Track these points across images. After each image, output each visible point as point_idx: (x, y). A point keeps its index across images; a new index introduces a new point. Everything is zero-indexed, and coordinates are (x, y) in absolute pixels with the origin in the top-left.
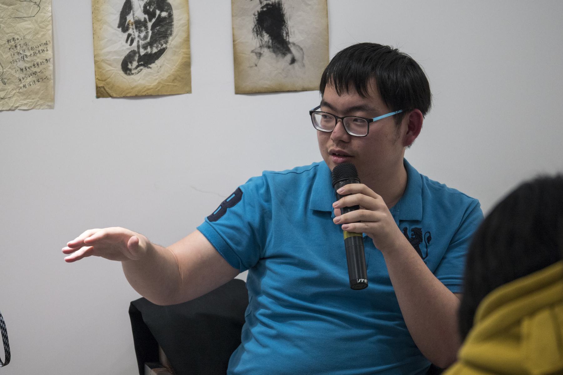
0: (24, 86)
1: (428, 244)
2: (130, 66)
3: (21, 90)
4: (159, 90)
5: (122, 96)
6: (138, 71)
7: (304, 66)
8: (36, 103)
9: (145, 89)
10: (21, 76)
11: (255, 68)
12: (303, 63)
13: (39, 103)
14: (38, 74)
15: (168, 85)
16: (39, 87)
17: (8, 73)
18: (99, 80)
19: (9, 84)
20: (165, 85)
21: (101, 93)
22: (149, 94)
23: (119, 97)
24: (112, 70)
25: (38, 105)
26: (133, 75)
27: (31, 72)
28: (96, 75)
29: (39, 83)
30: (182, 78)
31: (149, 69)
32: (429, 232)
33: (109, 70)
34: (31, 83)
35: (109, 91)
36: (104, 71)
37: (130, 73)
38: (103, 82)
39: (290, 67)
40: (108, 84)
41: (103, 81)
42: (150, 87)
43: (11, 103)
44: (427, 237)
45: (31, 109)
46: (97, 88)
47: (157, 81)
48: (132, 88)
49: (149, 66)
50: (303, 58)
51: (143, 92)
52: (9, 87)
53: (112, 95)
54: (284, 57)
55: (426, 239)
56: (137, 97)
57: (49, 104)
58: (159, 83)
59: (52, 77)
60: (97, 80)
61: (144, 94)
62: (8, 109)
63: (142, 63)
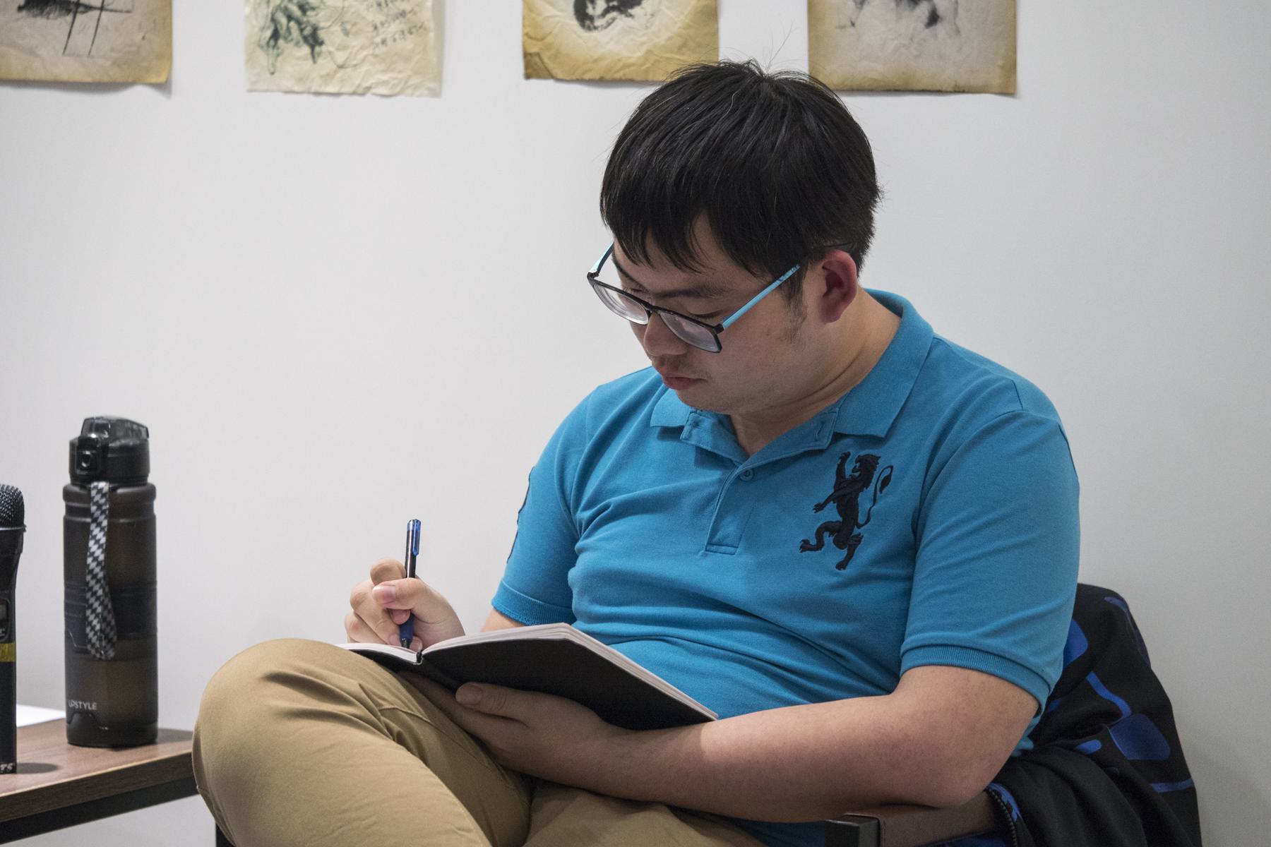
0: (384, 42)
1: (878, 493)
2: (590, 10)
3: (377, 51)
4: (648, 68)
5: (574, 78)
6: (607, 22)
7: (958, 32)
8: (406, 82)
9: (621, 64)
10: (379, 18)
11: (851, 30)
12: (955, 24)
13: (411, 82)
14: (409, 16)
15: (667, 59)
16: (410, 47)
17: (352, 10)
18: (531, 38)
19: (356, 34)
20: (661, 57)
21: (534, 68)
22: (629, 77)
23: (568, 79)
24: (556, 16)
25: (409, 86)
26: (596, 31)
27: (396, 11)
28: (524, 26)
29: (412, 36)
30: (699, 45)
31: (629, 19)
32: (892, 467)
33: (549, 17)
34: (397, 36)
35: (550, 65)
36: (539, 19)
37: (592, 26)
38: (540, 43)
39: (928, 31)
40: (549, 47)
41: (537, 39)
42: (632, 61)
43: (356, 78)
44: (885, 476)
45: (396, 95)
46: (527, 55)
47: (644, 49)
48: (596, 61)
49: (630, 11)
50: (956, 11)
51: (618, 71)
52: (355, 42)
53: (554, 75)
54: (914, 8)
55: (880, 482)
56: (602, 82)
57: (432, 85)
58: (649, 52)
59: (431, 24)
60: (526, 38)
61: (618, 76)
62: (351, 90)
63: (615, 3)
